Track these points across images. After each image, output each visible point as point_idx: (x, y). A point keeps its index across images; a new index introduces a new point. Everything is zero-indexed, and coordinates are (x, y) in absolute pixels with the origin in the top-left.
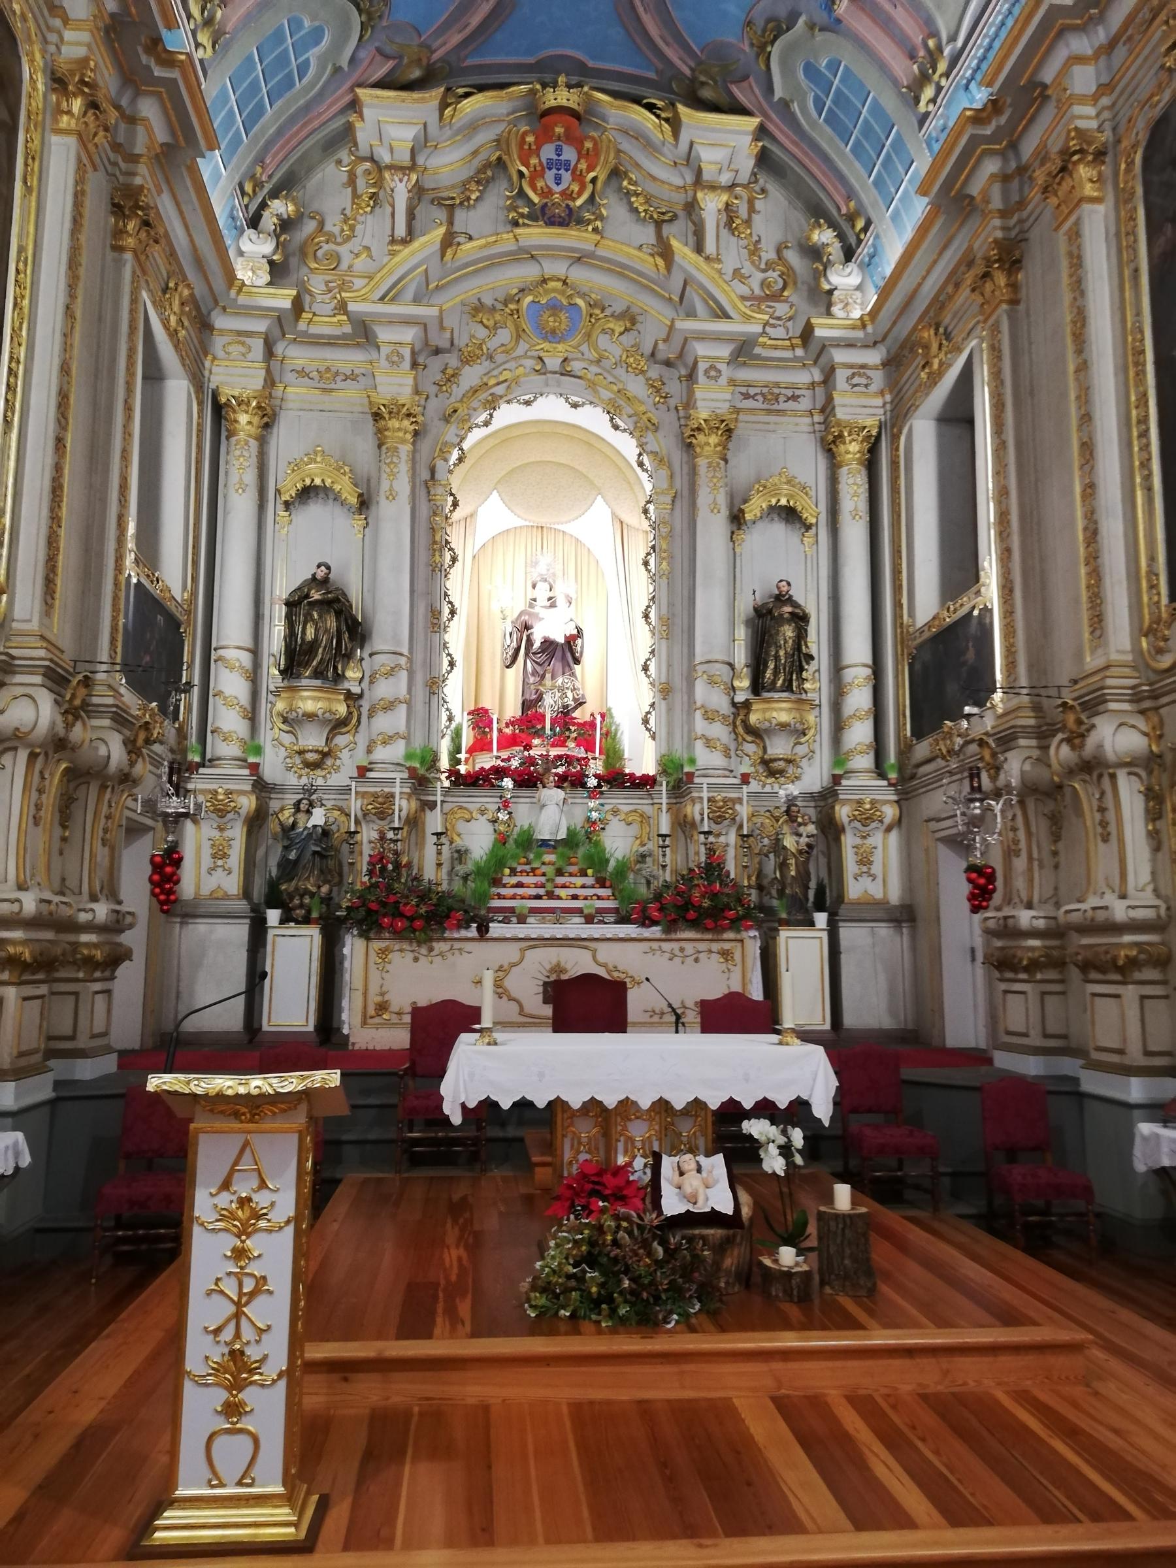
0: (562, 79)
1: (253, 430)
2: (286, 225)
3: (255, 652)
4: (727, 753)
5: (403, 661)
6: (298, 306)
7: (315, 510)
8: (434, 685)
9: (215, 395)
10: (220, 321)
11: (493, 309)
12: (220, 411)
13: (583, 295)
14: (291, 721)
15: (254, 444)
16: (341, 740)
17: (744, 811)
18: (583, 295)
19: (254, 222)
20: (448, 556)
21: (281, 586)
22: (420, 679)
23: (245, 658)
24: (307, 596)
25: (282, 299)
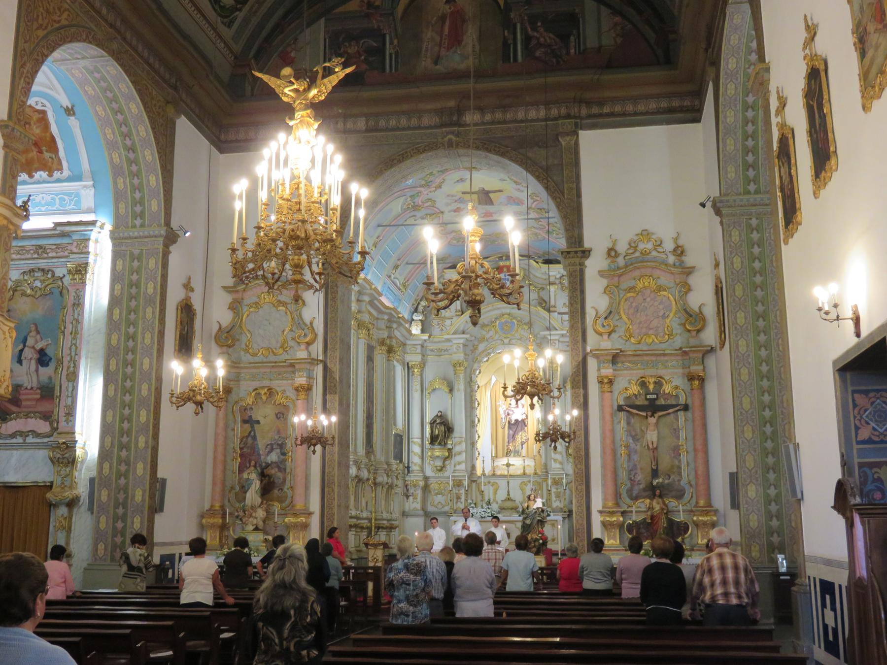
0: (504, 258)
1: (418, 373)
2: (424, 307)
3: (422, 438)
4: (561, 463)
5: (463, 440)
6: (430, 337)
7: (437, 392)
8: (473, 444)
9: (408, 364)
10: (408, 342)
11: (488, 325)
12: (408, 367)
13: (514, 318)
14: (433, 458)
15: (419, 377)
16: (447, 462)
17: (564, 481)
18: (514, 318)
19: (416, 310)
20: (477, 403)
21: (428, 419)
22: (469, 442)
23: (419, 441)
24: (436, 421)
25: (425, 337)
